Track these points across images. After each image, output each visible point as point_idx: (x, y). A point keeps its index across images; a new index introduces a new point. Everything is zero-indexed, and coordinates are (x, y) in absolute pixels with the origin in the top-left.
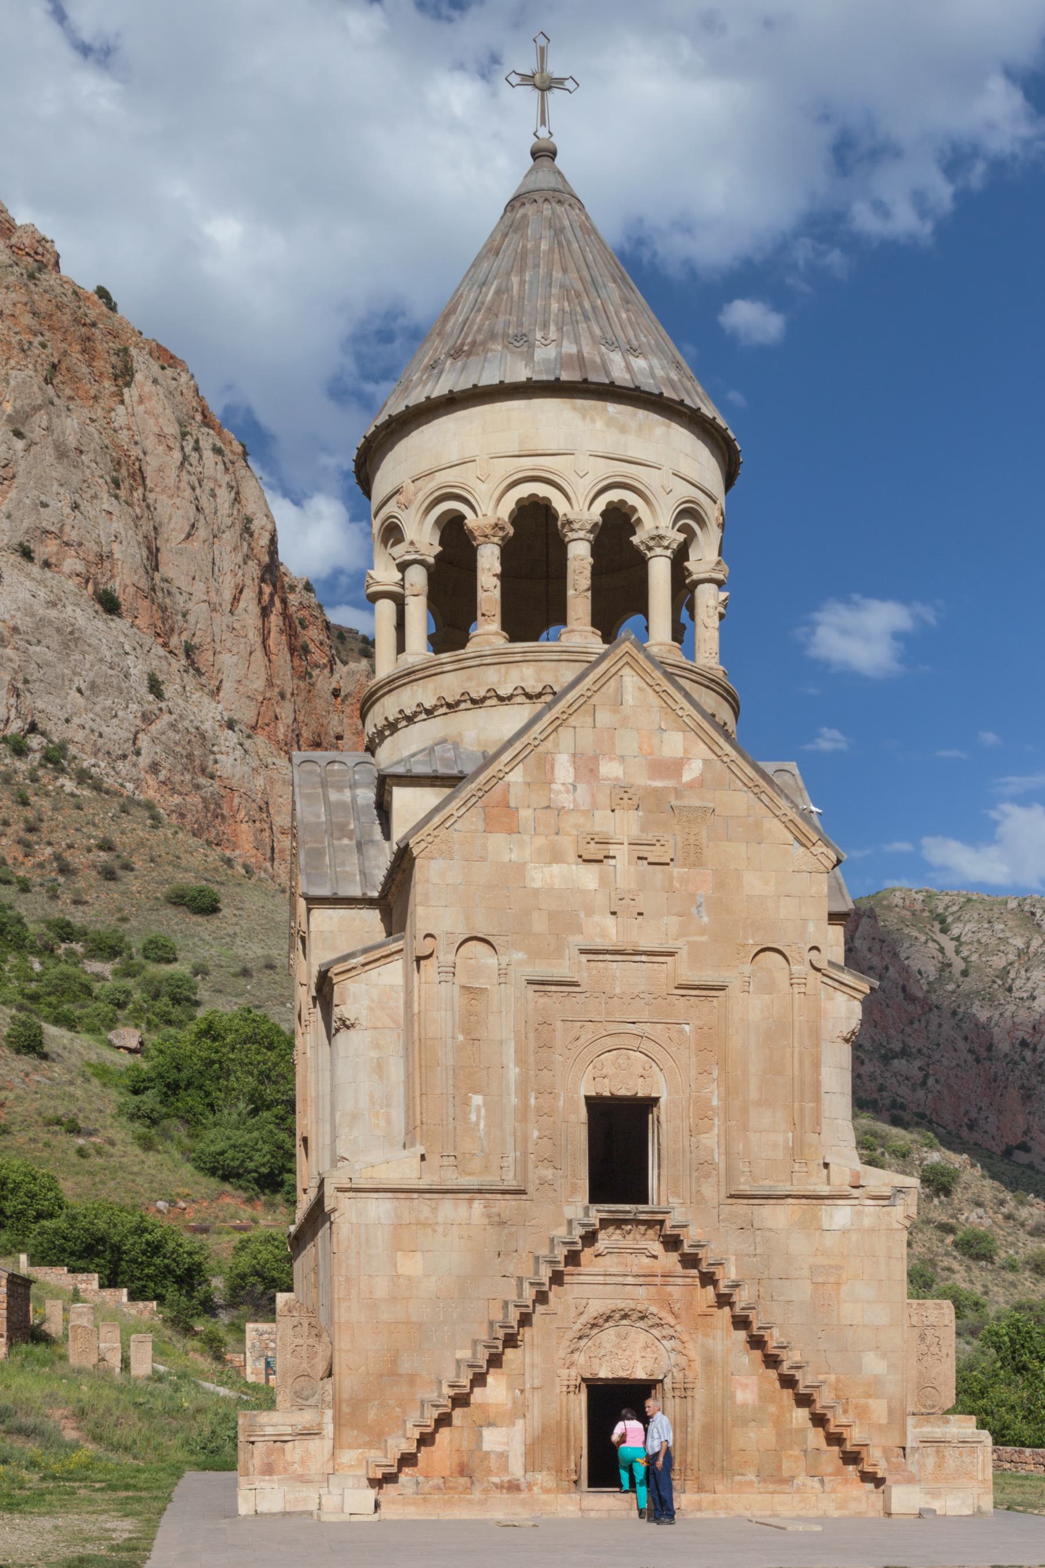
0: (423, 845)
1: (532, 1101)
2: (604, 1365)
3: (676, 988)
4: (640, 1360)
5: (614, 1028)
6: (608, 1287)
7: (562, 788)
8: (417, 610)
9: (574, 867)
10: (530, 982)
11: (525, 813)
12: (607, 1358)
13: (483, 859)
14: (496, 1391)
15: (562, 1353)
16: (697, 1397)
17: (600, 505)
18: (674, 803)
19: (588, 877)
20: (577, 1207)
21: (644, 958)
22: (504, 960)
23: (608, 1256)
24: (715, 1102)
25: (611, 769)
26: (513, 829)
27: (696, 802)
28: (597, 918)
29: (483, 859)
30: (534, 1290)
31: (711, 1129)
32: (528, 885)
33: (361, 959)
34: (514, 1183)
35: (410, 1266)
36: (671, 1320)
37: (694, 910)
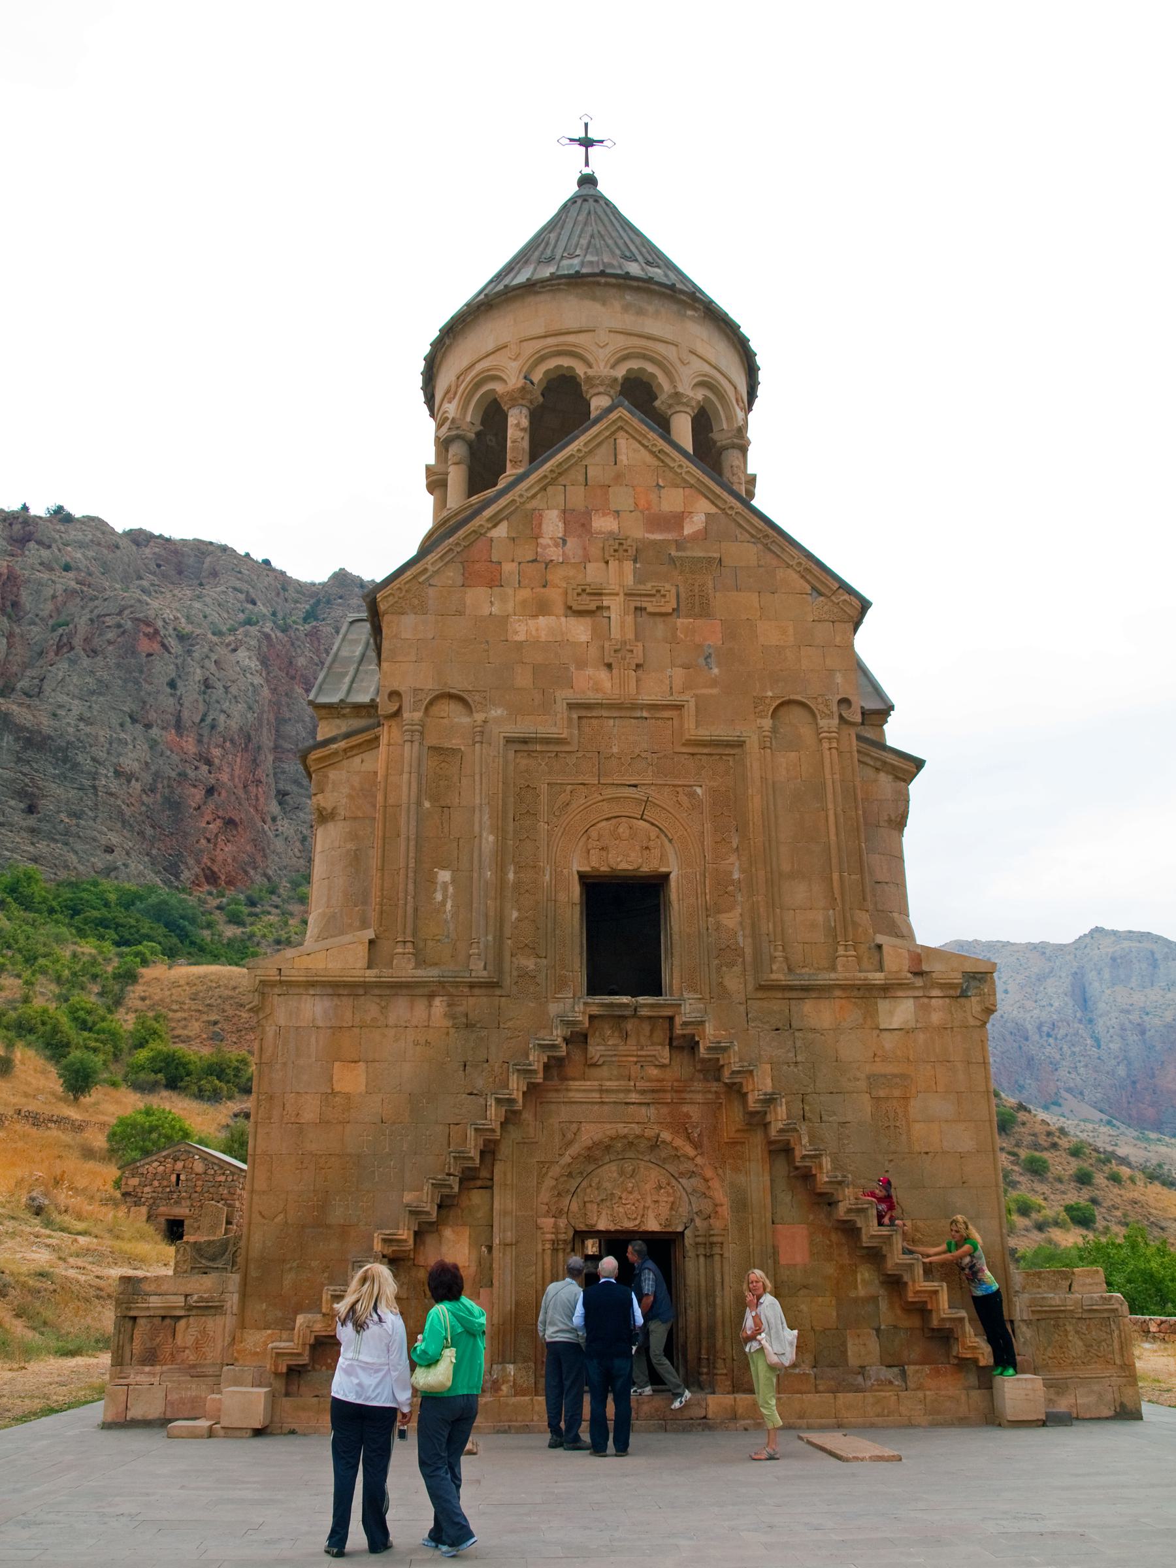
0: (391, 600)
1: (511, 876)
2: (604, 1212)
3: (684, 745)
4: (652, 1206)
5: (609, 792)
6: (606, 1107)
7: (550, 542)
9: (563, 619)
11: (508, 568)
12: (608, 1204)
13: (460, 613)
15: (545, 1196)
16: (726, 1255)
18: (673, 553)
19: (580, 630)
22: (479, 717)
23: (605, 1068)
24: (736, 876)
25: (603, 524)
26: (494, 581)
27: (699, 553)
28: (590, 671)
30: (504, 1109)
31: (731, 908)
33: (342, 744)
34: (485, 973)
36: (690, 1151)
37: (701, 661)
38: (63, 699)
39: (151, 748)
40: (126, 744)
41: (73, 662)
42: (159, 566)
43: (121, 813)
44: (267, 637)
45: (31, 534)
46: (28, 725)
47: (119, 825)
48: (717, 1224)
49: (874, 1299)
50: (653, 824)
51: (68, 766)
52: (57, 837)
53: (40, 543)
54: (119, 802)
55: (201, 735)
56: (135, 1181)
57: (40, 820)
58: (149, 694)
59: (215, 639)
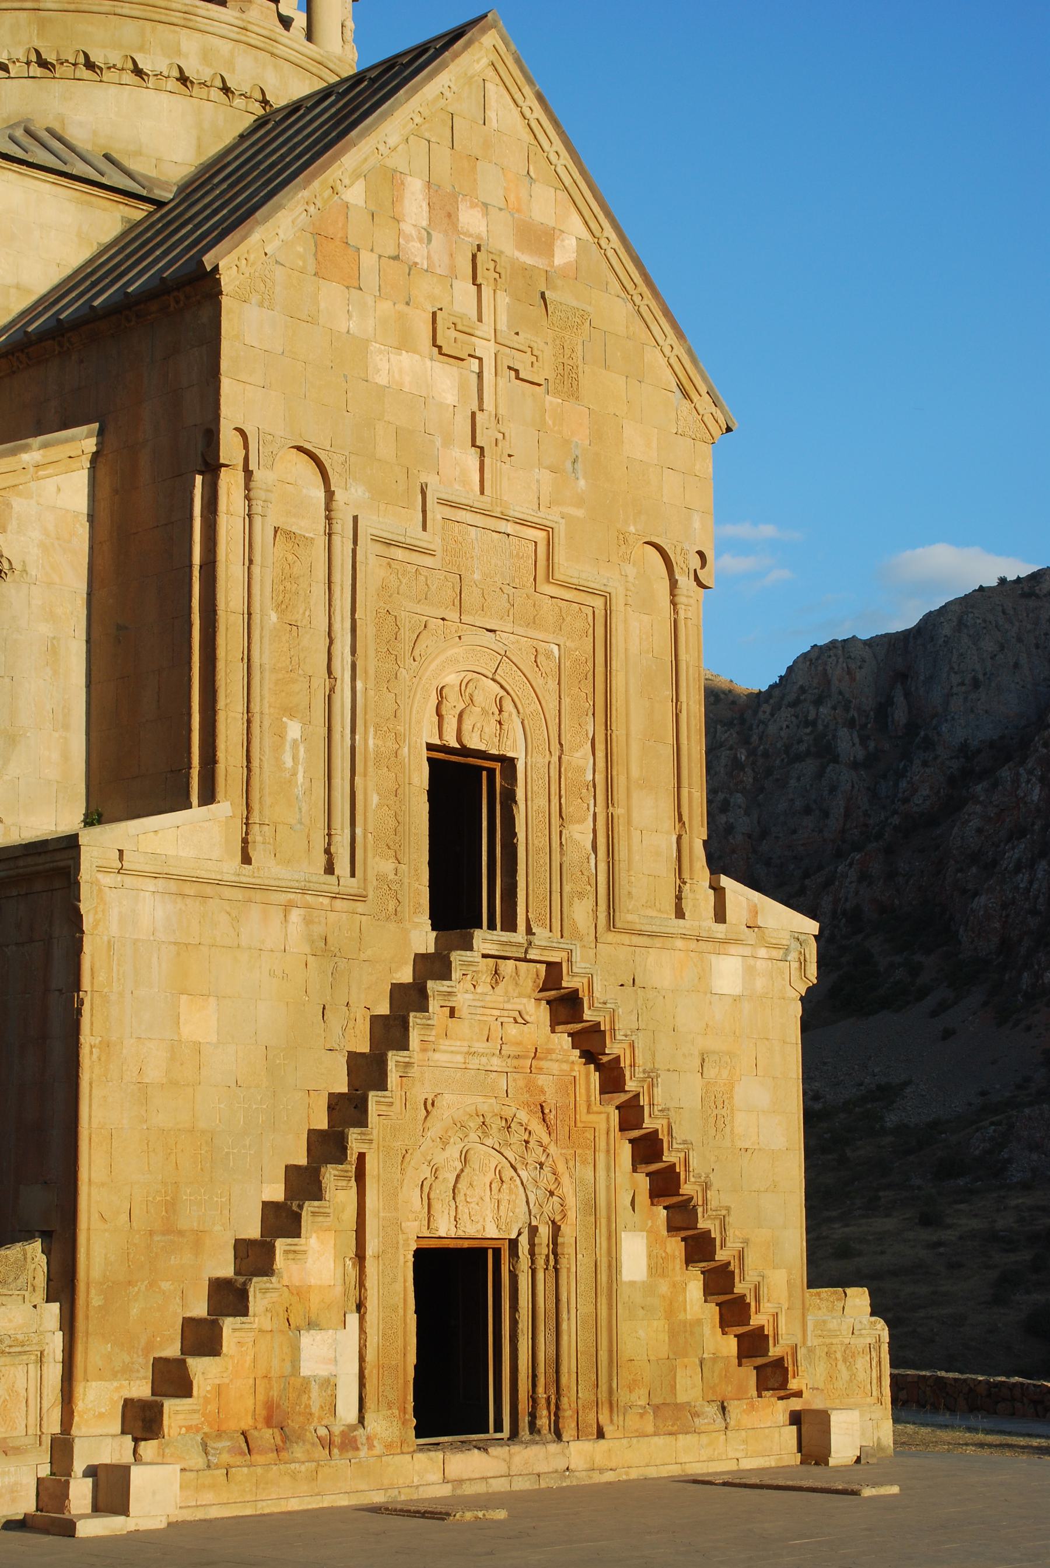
7: (414, 233)
9: (428, 363)
11: (368, 260)
19: (446, 384)
21: (510, 528)
28: (456, 452)
29: (312, 320)
32: (370, 378)
37: (568, 465)
48: (568, 1233)
49: (699, 1322)
50: (502, 687)
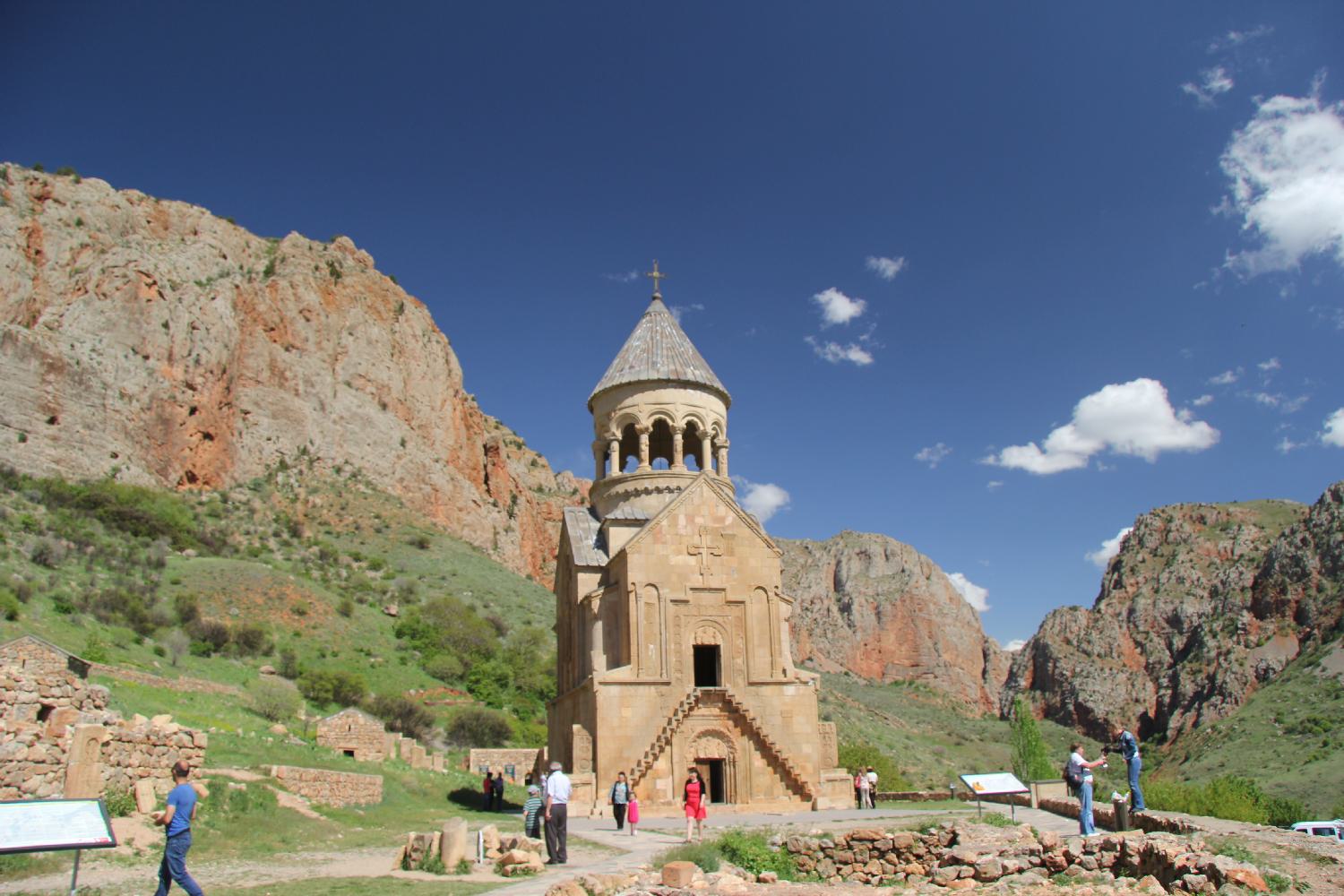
8: (615, 457)
10: (672, 601)
14: (661, 764)
17: (685, 421)
19: (692, 560)
20: (690, 686)
25: (699, 520)
35: (627, 713)
38: (77, 332)
39: (150, 375)
40: (129, 371)
41: (87, 303)
42: (149, 222)
43: (125, 427)
44: (237, 287)
45: (49, 193)
46: (51, 353)
47: (123, 436)
48: (736, 755)
51: (83, 387)
52: (75, 444)
53: (56, 201)
54: (124, 418)
55: (187, 366)
56: (326, 729)
57: (60, 430)
58: (148, 332)
59: (197, 288)
